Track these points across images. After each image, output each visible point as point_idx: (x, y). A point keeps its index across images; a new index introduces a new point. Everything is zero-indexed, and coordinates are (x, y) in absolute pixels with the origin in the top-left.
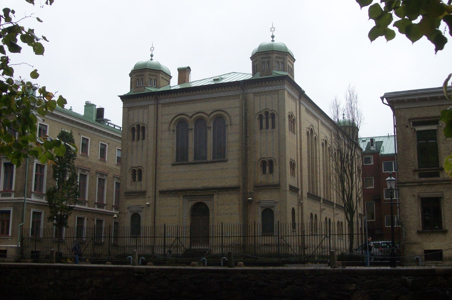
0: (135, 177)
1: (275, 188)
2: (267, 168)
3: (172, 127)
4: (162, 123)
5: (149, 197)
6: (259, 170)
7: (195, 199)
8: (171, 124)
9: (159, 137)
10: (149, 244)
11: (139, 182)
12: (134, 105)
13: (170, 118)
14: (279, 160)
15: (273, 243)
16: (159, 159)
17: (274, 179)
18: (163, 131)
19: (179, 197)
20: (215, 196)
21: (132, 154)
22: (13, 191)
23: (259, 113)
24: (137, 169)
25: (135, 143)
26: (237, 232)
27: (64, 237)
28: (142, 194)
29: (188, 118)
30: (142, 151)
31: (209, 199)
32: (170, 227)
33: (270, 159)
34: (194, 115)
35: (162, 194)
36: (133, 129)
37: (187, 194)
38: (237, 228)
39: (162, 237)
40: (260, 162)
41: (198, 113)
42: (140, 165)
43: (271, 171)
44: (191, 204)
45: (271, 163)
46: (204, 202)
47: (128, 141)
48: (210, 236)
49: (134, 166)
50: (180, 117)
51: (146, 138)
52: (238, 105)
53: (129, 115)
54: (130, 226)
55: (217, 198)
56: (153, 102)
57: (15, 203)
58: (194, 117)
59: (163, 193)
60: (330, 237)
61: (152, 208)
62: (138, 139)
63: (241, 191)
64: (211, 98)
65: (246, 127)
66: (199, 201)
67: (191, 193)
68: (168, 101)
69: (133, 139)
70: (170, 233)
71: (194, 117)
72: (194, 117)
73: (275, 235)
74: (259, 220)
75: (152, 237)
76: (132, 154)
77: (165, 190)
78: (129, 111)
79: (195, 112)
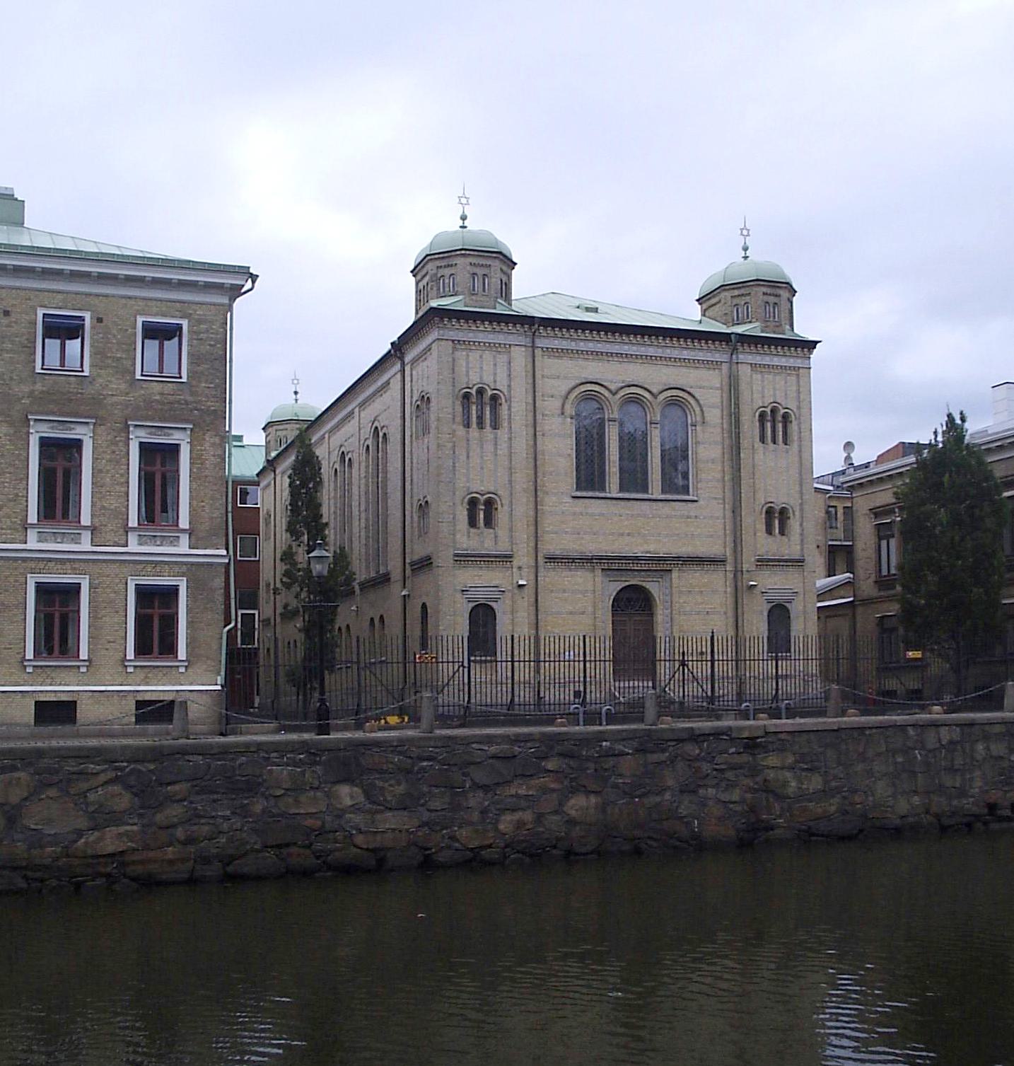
3: (570, 410)
7: (624, 579)
12: (471, 336)
13: (564, 387)
14: (802, 510)
18: (546, 415)
19: (593, 570)
20: (675, 574)
21: (468, 457)
22: (184, 531)
25: (474, 432)
28: (507, 558)
29: (606, 393)
33: (784, 505)
34: (622, 388)
39: (579, 661)
42: (492, 489)
44: (616, 587)
45: (783, 513)
46: (644, 584)
47: (454, 427)
49: (475, 490)
56: (522, 340)
57: (192, 564)
59: (551, 559)
61: (529, 592)
62: (481, 424)
63: (729, 568)
68: (556, 343)
70: (572, 653)
71: (622, 393)
72: (622, 393)
73: (793, 658)
77: (558, 552)
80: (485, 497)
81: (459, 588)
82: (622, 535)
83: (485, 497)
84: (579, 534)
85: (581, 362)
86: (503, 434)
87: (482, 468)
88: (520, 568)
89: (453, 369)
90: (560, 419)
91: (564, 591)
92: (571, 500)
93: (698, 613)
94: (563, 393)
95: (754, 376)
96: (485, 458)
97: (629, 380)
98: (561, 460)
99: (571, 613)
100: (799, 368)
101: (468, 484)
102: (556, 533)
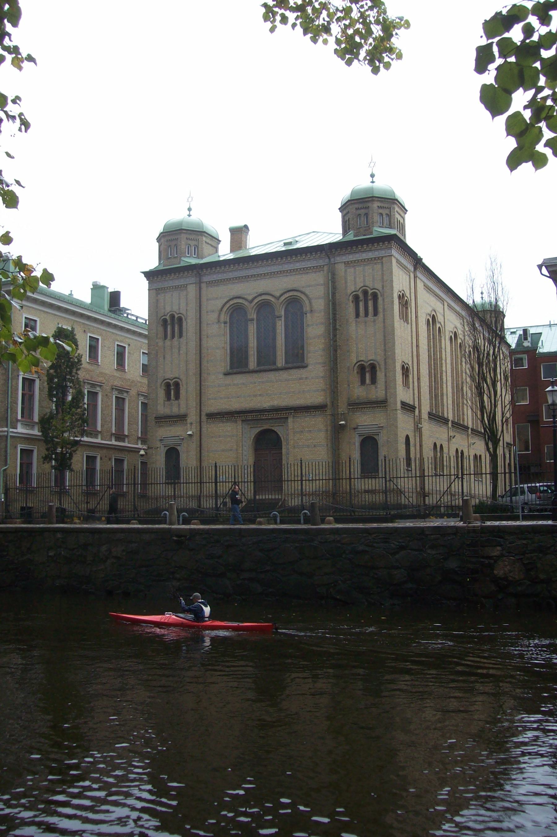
0: (170, 393)
1: (380, 406)
2: (368, 376)
4: (207, 312)
5: (191, 424)
6: (355, 378)
7: (259, 426)
9: (203, 333)
10: (193, 494)
11: (177, 402)
12: (166, 285)
13: (219, 303)
14: (385, 363)
15: (377, 488)
16: (205, 366)
17: (378, 392)
20: (290, 420)
21: (164, 358)
23: (354, 293)
24: (171, 382)
25: (168, 342)
26: (324, 473)
27: (67, 485)
28: (181, 418)
29: (246, 303)
30: (179, 354)
31: (280, 424)
32: (224, 468)
33: (372, 362)
34: (256, 297)
35: (210, 418)
36: (165, 321)
37: (248, 417)
38: (324, 466)
39: (212, 482)
40: (356, 368)
41: (261, 295)
42: (177, 376)
43: (374, 381)
45: (373, 368)
46: (273, 428)
47: (157, 340)
48: (283, 480)
50: (235, 301)
51: (184, 334)
52: (322, 282)
53: (157, 300)
54: (164, 467)
55: (293, 422)
56: (193, 280)
58: (256, 302)
59: (211, 416)
60: (462, 478)
61: (196, 438)
63: (329, 412)
64: (281, 271)
65: (334, 314)
66: (266, 427)
67: (253, 415)
68: (215, 277)
69: (166, 337)
70: (224, 477)
71: (256, 301)
72: (256, 301)
73: (380, 476)
74: (356, 455)
75: (198, 483)
76: (164, 358)
77: (216, 411)
78: (157, 294)
79: (257, 293)
81: (159, 438)
86: (183, 340)
88: (191, 424)
89: (157, 306)
91: (220, 436)
93: (308, 446)
95: (348, 270)
97: (260, 291)
98: (218, 351)
99: (223, 451)
100: (382, 257)
102: (215, 399)
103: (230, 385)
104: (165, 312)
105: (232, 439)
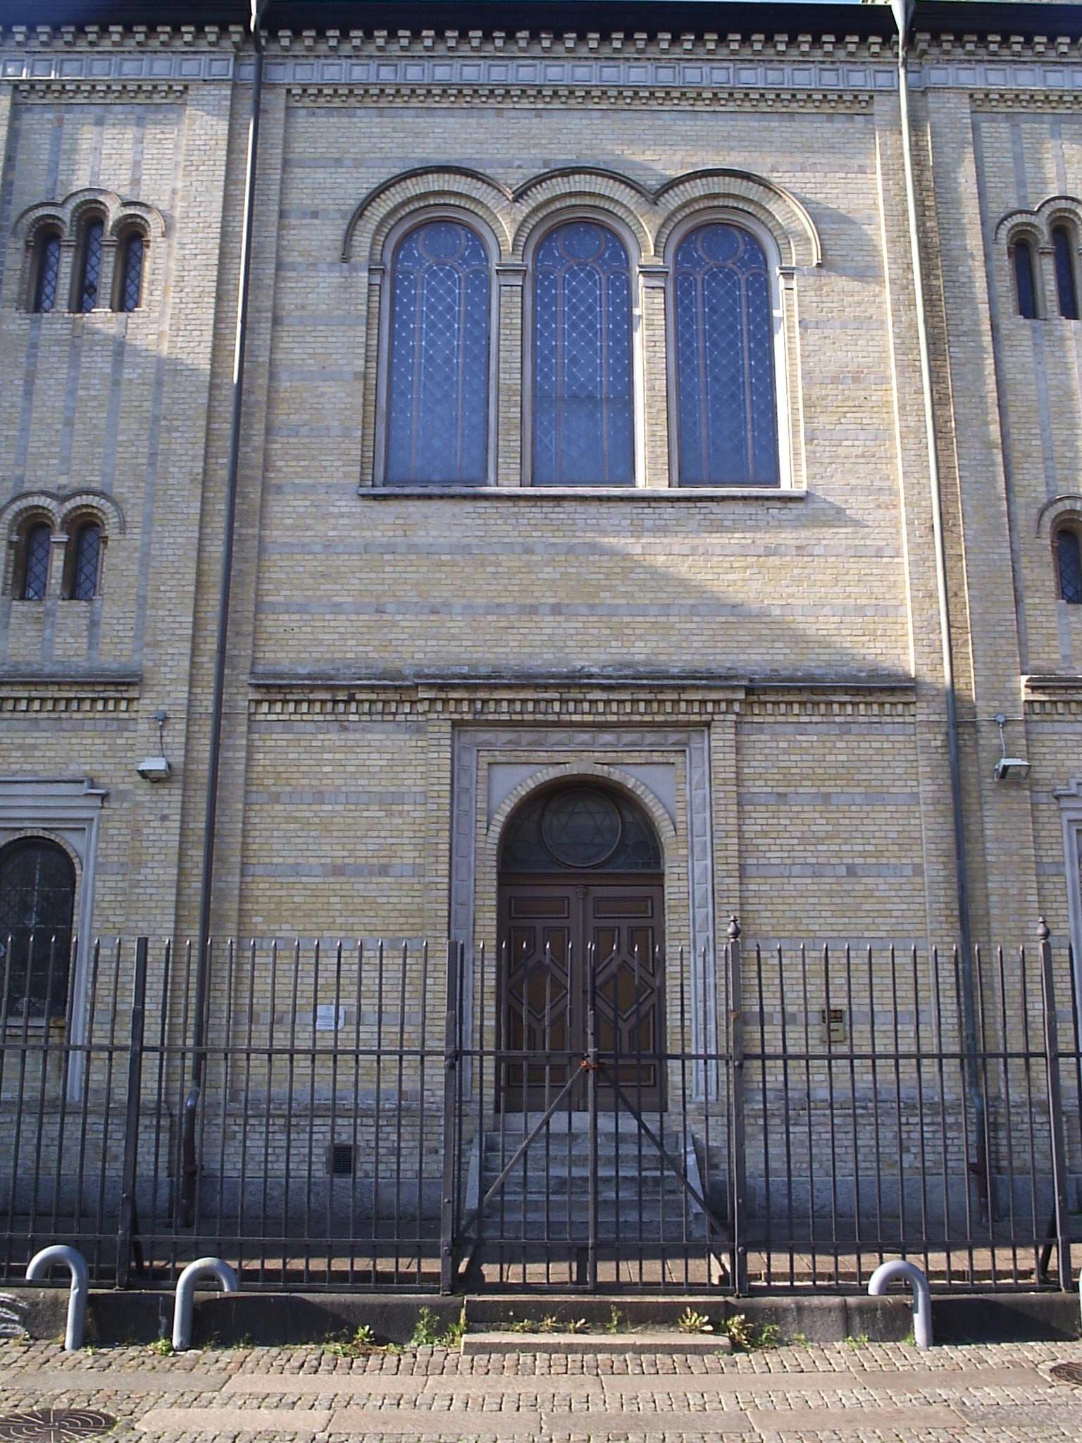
8: (361, 223)
11: (81, 606)
13: (356, 186)
16: (255, 449)
20: (722, 738)
21: (28, 393)
24: (58, 512)
25: (58, 320)
31: (656, 757)
35: (272, 702)
37: (492, 705)
42: (95, 481)
46: (616, 774)
49: (40, 486)
56: (222, 67)
67: (524, 701)
76: (28, 393)
79: (546, 163)
80: (69, 505)
82: (533, 610)
83: (69, 505)
84: (380, 611)
85: (409, 120)
87: (69, 422)
90: (335, 278)
91: (319, 797)
92: (358, 506)
93: (817, 872)
94: (352, 204)
96: (81, 393)
97: (565, 157)
98: (328, 388)
99: (338, 870)
101: (18, 472)
102: (302, 609)
103: (391, 549)
104: (53, 190)
105: (390, 814)
